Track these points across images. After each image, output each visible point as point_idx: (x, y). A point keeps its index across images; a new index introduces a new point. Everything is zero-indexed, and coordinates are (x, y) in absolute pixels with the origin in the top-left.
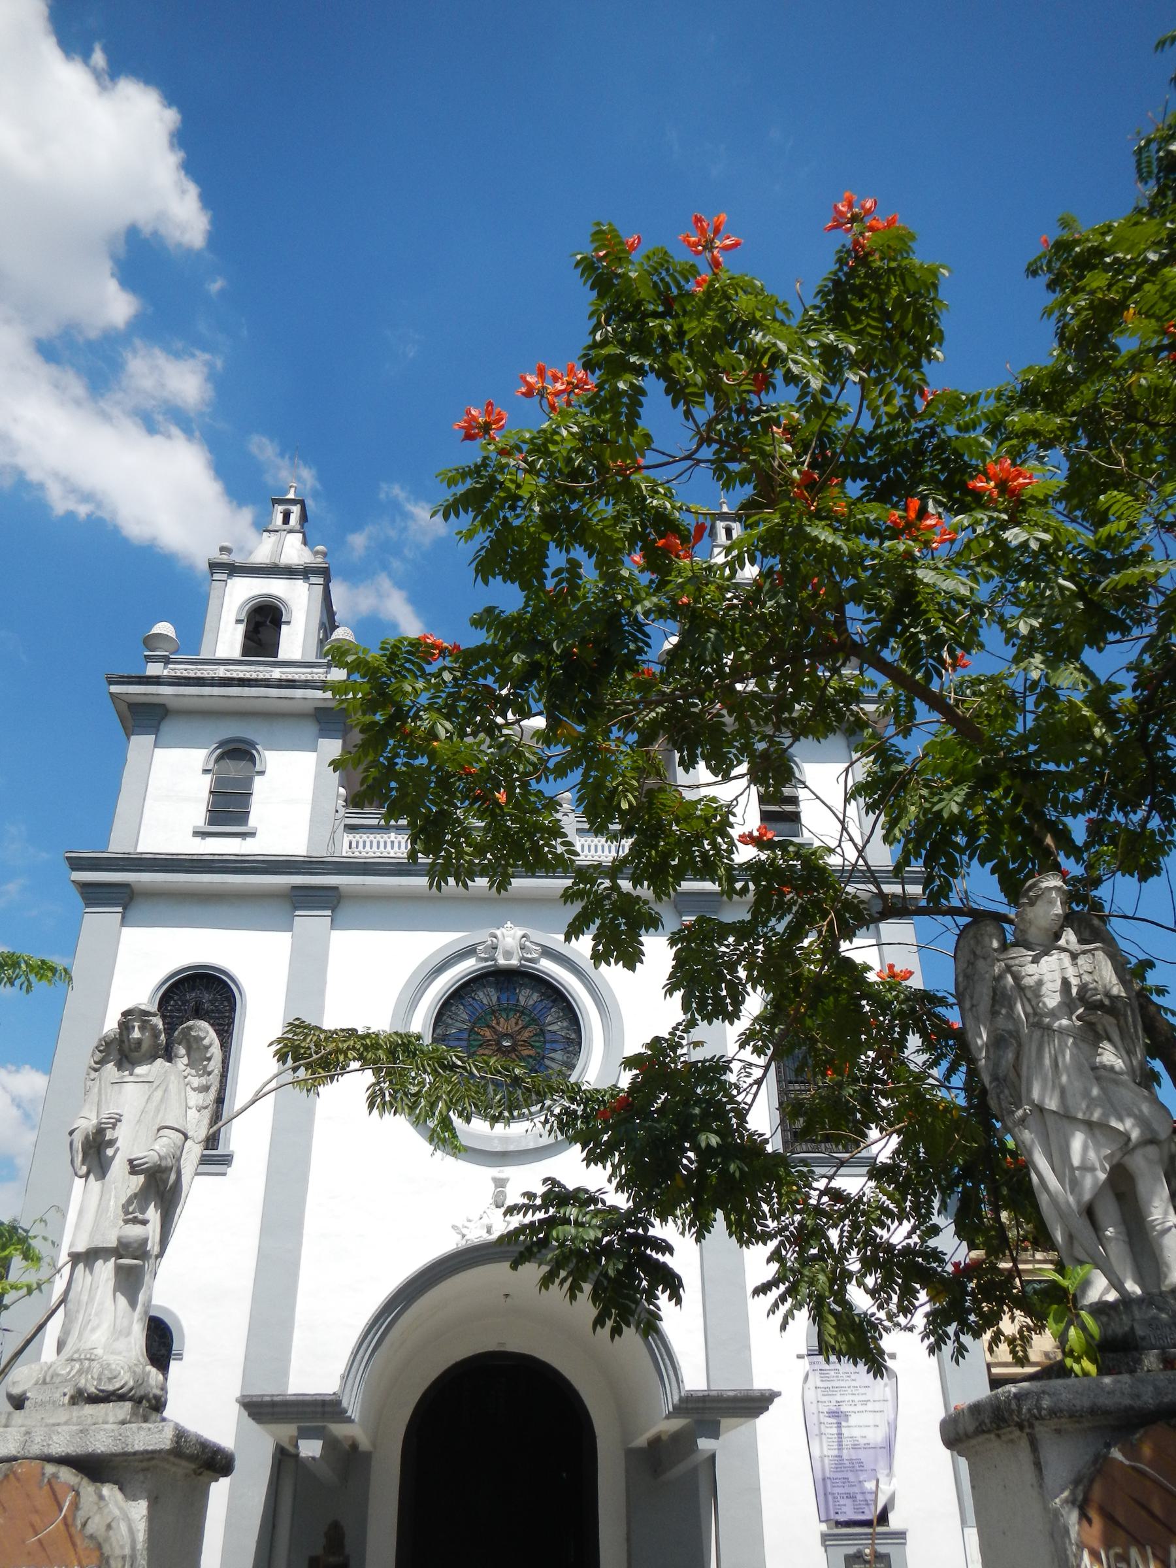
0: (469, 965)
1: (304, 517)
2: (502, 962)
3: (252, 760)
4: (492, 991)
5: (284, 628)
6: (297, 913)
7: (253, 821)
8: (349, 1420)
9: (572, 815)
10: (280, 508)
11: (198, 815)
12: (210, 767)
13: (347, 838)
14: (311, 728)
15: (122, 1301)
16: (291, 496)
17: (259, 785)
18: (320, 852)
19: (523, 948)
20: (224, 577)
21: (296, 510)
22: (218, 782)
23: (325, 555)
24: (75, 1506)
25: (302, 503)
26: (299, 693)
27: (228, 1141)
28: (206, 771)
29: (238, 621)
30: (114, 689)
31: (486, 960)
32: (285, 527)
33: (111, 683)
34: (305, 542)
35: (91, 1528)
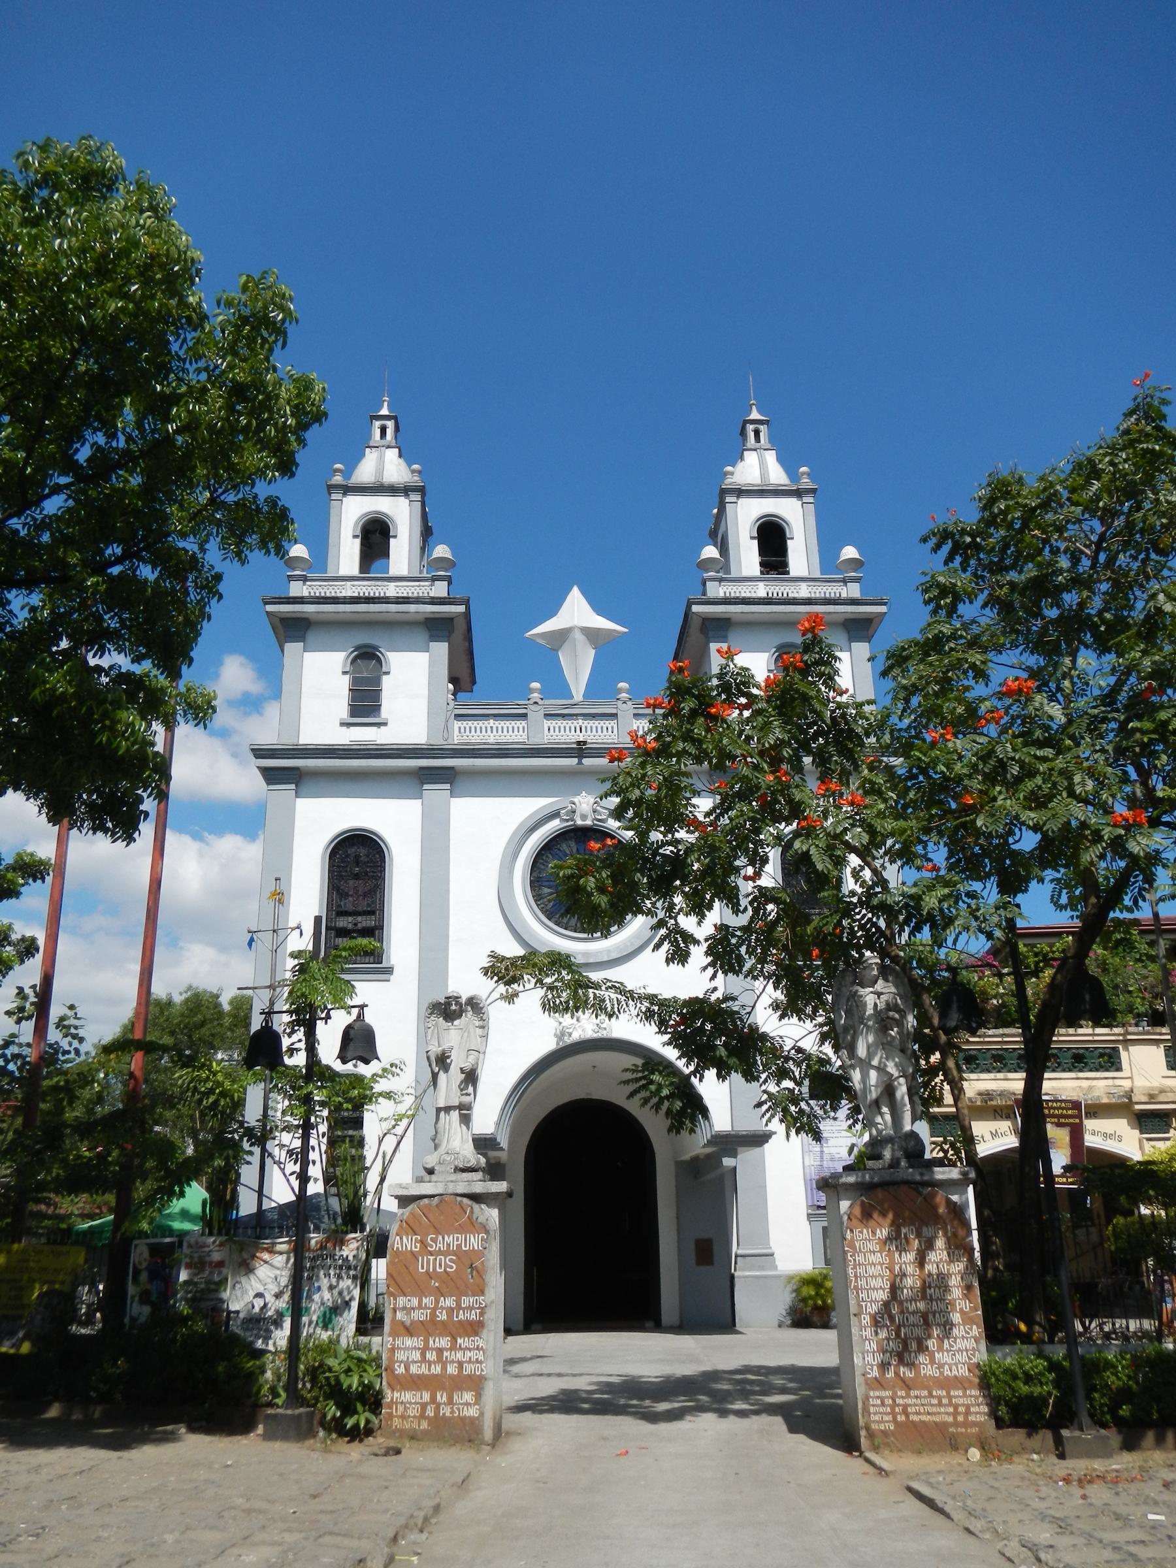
0: (554, 825)
1: (397, 429)
2: (579, 822)
3: (379, 661)
4: (573, 844)
5: (392, 540)
6: (426, 787)
7: (385, 712)
8: (502, 1149)
9: (630, 703)
10: (377, 424)
11: (342, 709)
12: (347, 669)
13: (457, 724)
14: (422, 635)
15: (464, 1127)
16: (384, 411)
17: (385, 678)
18: (438, 741)
19: (595, 811)
20: (339, 496)
21: (390, 424)
22: (355, 681)
23: (420, 472)
24: (472, 1212)
25: (395, 418)
26: (412, 608)
27: (389, 957)
28: (345, 673)
29: (355, 537)
30: (269, 608)
31: (567, 821)
32: (383, 442)
33: (266, 603)
34: (400, 456)
35: (480, 1220)
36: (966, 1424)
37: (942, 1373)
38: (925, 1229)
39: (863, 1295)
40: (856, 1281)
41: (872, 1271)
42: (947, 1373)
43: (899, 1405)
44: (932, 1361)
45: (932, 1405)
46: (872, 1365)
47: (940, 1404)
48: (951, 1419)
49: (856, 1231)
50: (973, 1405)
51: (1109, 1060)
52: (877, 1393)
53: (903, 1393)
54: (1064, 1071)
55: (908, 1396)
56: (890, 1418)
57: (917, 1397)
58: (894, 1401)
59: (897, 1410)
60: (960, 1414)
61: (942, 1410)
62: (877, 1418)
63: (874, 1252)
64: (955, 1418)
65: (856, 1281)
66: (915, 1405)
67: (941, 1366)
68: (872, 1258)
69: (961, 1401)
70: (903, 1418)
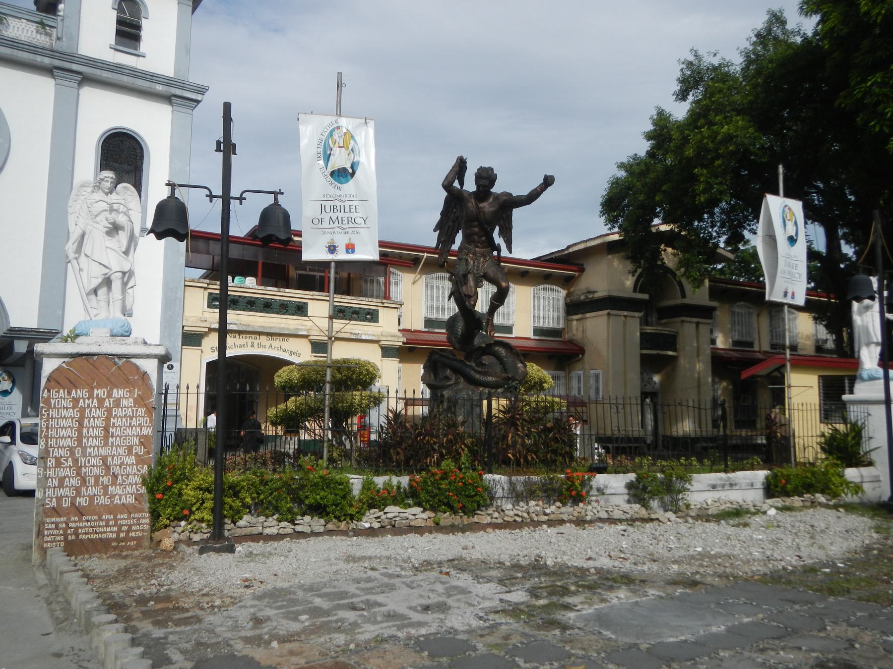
36: (127, 539)
37: (112, 502)
38: (115, 390)
39: (52, 442)
40: (47, 431)
41: (63, 423)
42: (117, 501)
43: (71, 528)
44: (106, 493)
45: (100, 526)
46: (52, 498)
47: (107, 526)
48: (115, 535)
49: (53, 392)
50: (134, 525)
51: (301, 310)
52: (53, 520)
53: (76, 519)
54: (274, 313)
55: (80, 521)
56: (62, 538)
57: (88, 521)
58: (67, 524)
59: (69, 532)
60: (123, 532)
61: (108, 529)
62: (49, 539)
63: (67, 408)
64: (118, 535)
65: (47, 431)
66: (85, 527)
67: (112, 497)
68: (64, 413)
69: (124, 522)
70: (74, 537)
